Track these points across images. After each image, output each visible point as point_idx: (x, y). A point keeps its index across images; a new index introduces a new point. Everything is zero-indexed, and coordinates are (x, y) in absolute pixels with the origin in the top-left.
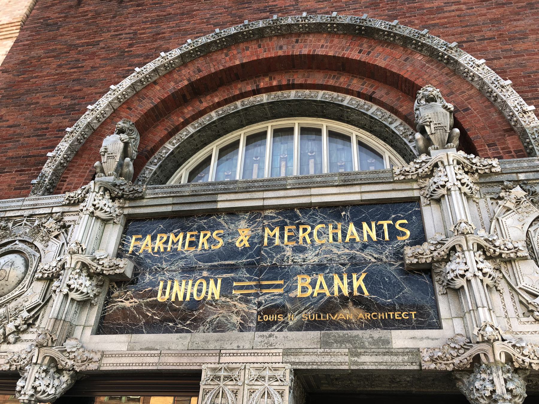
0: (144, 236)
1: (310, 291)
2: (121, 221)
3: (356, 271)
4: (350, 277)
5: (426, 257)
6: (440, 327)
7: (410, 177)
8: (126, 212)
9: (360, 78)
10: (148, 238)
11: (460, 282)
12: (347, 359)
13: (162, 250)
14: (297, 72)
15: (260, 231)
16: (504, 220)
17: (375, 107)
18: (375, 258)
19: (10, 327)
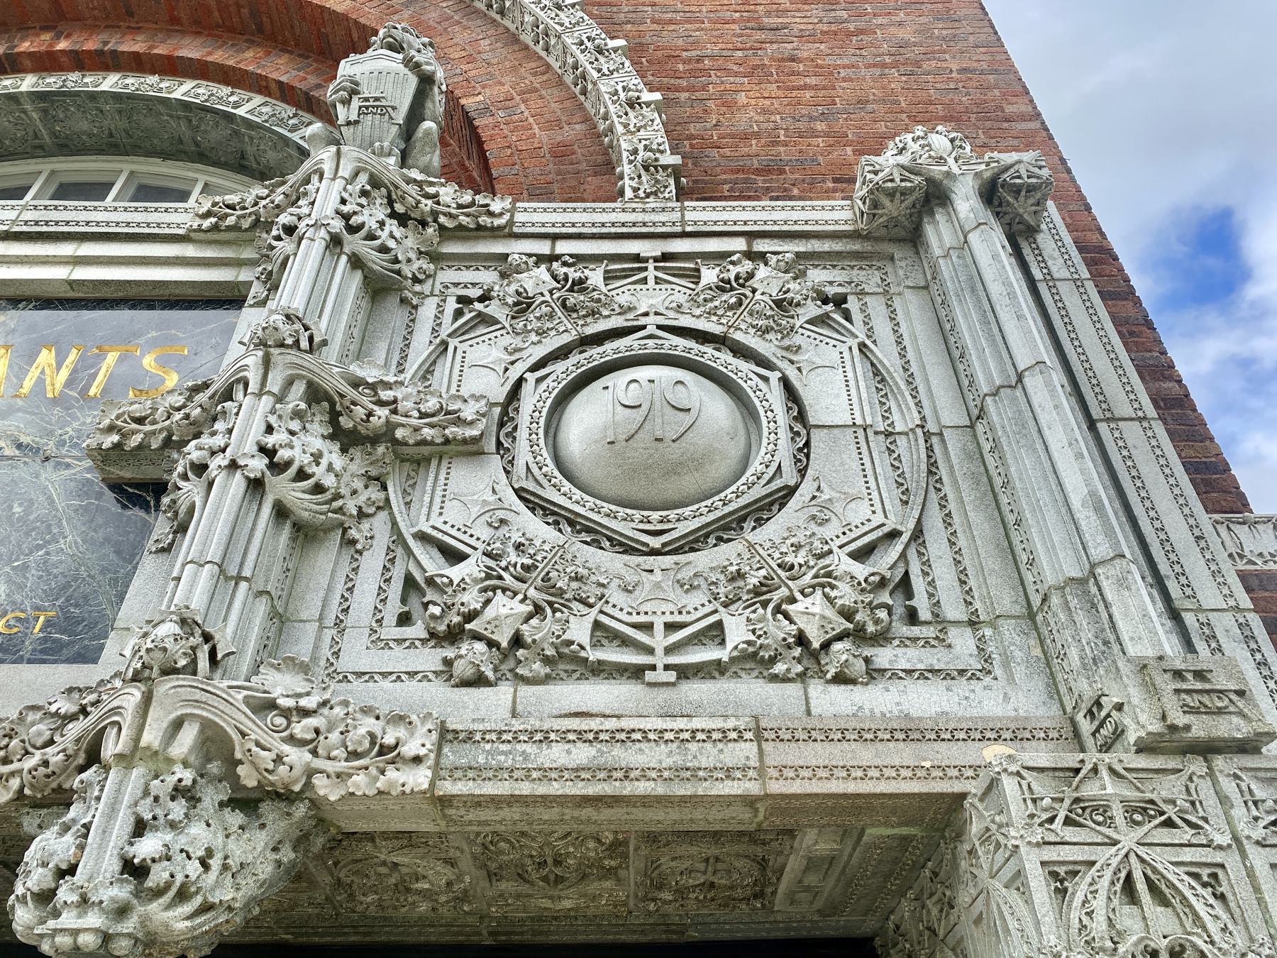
5: (148, 428)
7: (231, 221)
9: (300, 56)
14: (139, 28)
16: (461, 347)
18: (20, 446)
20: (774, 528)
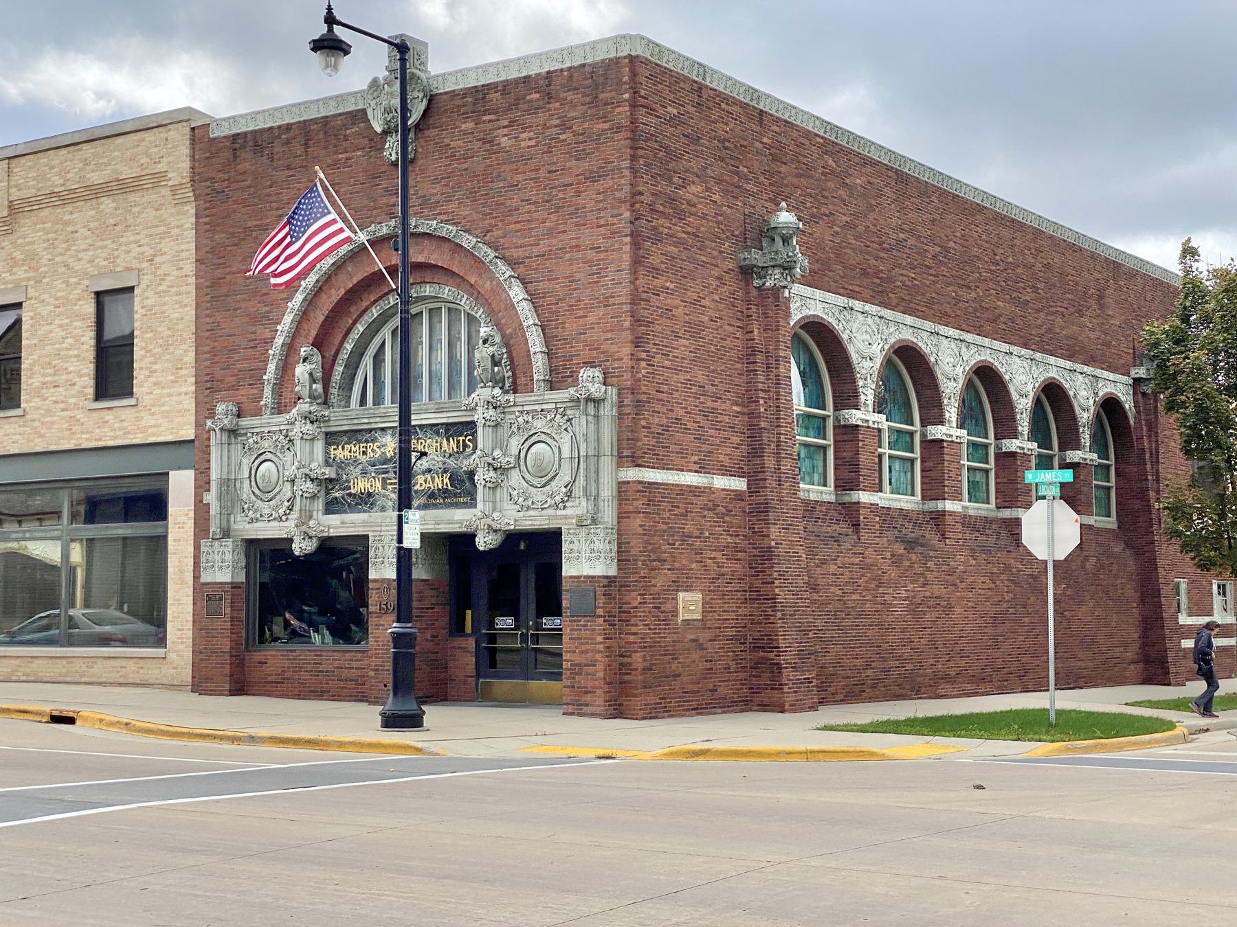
2: (322, 436)
19: (281, 511)
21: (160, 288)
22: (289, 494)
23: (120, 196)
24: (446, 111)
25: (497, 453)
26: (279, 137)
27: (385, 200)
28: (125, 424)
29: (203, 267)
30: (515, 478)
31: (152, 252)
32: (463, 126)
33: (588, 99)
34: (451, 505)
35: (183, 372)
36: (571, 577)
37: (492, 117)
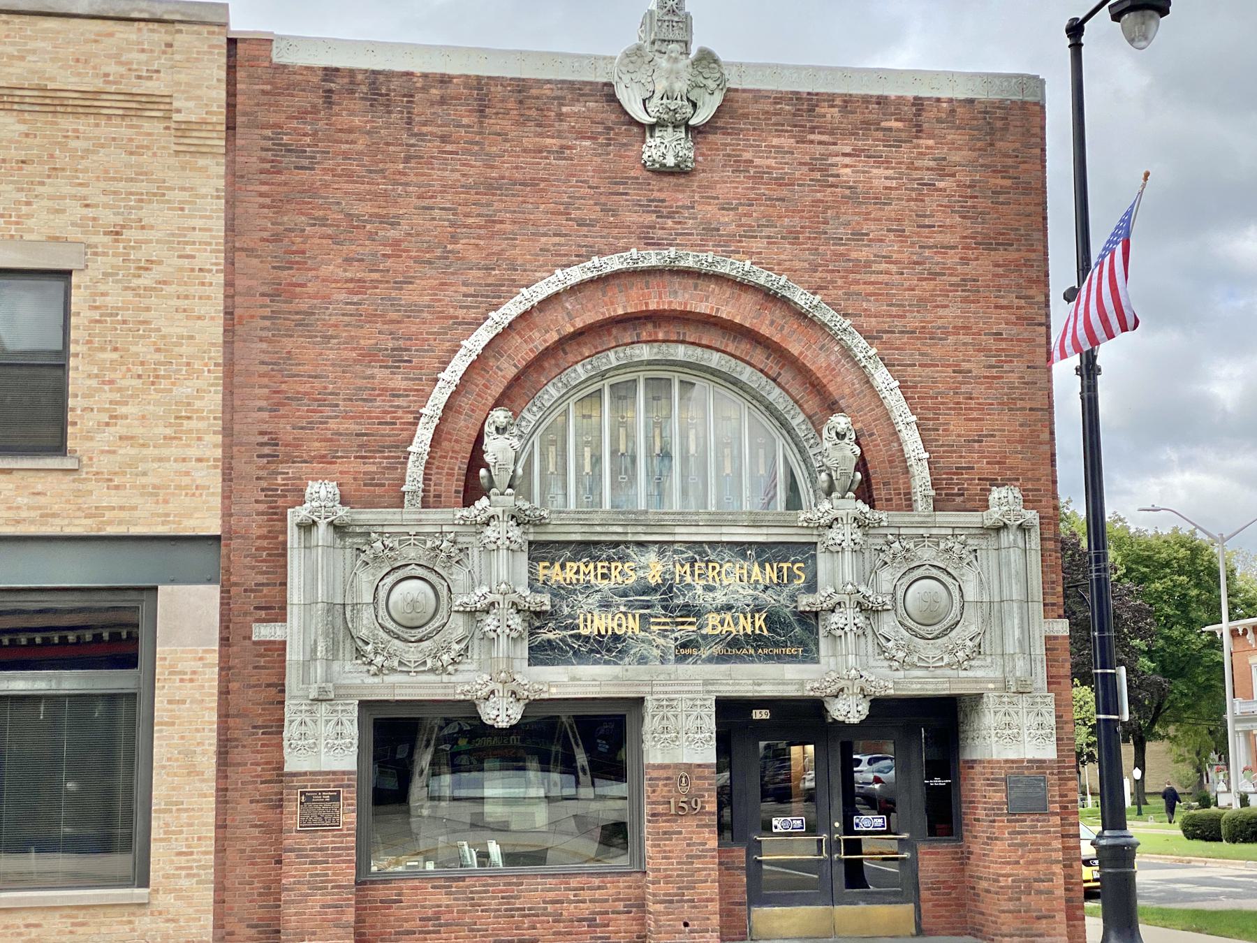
0: (552, 564)
1: (720, 628)
2: (525, 547)
3: (759, 611)
4: (753, 617)
6: (818, 662)
8: (531, 538)
10: (557, 565)
11: (839, 632)
12: (750, 688)
13: (574, 581)
15: (671, 567)
17: (778, 391)
19: (446, 658)
20: (953, 633)
21: (135, 282)
22: (460, 632)
23: (42, 117)
24: (746, 116)
25: (862, 589)
26: (424, 89)
27: (635, 218)
28: (42, 500)
29: (255, 261)
30: (888, 625)
31: (119, 220)
32: (775, 141)
33: (979, 144)
34: (769, 658)
35: (193, 424)
36: (1006, 761)
37: (825, 138)
